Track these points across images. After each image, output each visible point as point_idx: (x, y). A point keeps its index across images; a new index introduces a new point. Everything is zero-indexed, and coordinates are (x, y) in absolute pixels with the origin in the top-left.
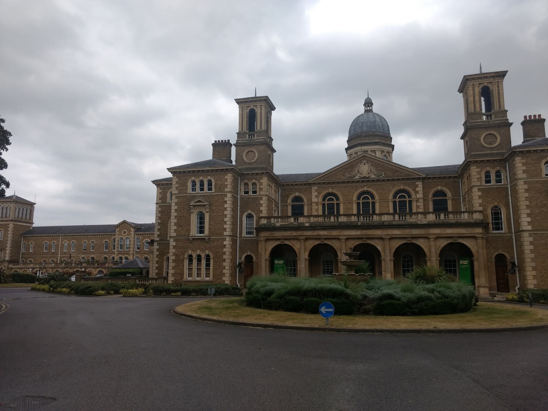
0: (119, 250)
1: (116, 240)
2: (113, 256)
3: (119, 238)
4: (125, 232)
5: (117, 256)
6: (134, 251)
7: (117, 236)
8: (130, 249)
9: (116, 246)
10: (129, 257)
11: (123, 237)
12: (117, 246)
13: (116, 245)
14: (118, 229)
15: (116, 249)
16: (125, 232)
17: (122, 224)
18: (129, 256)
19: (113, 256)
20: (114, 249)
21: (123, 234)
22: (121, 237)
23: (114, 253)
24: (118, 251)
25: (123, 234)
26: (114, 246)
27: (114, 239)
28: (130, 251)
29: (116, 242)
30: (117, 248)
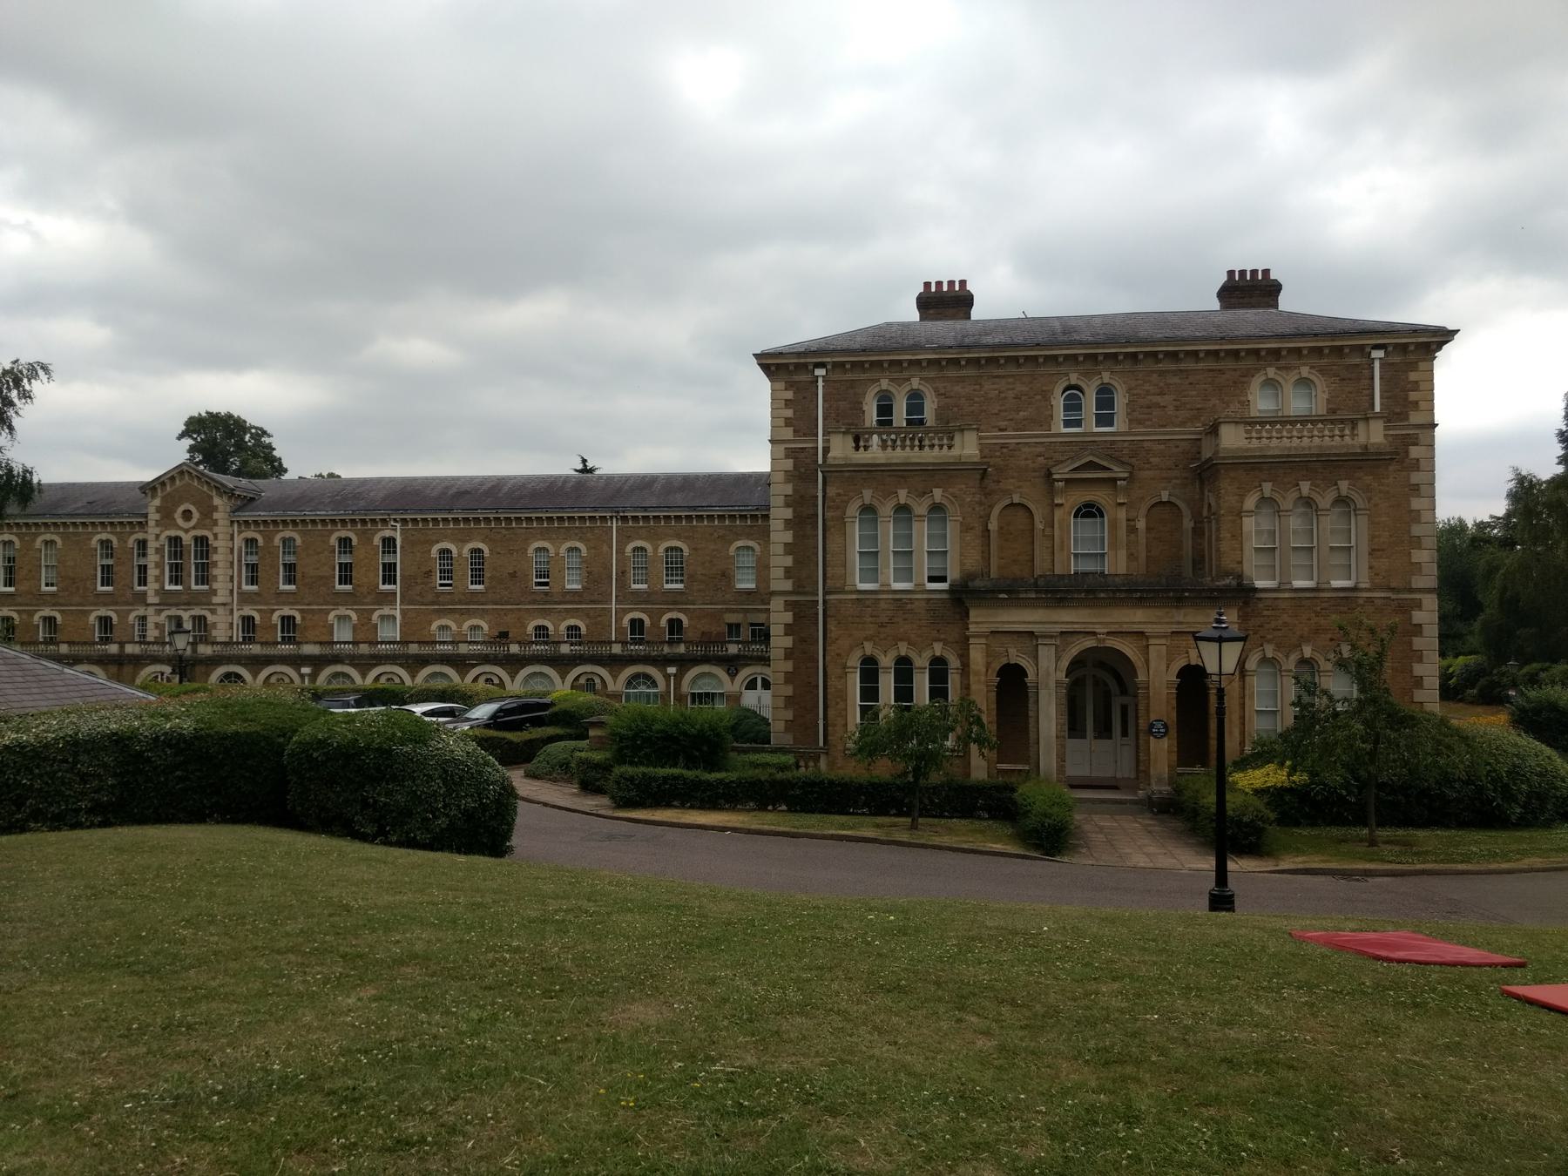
0: (194, 587)
1: (152, 545)
2: (141, 611)
3: (163, 537)
4: (187, 515)
5: (159, 612)
6: (232, 591)
7: (152, 530)
8: (215, 586)
9: (152, 572)
10: (210, 618)
11: (181, 534)
12: (157, 572)
13: (151, 566)
14: (157, 502)
15: (152, 586)
16: (187, 515)
17: (172, 479)
18: (213, 612)
19: (141, 611)
20: (143, 581)
21: (180, 522)
22: (173, 533)
23: (141, 599)
24: (161, 592)
25: (180, 522)
26: (143, 569)
27: (143, 544)
28: (214, 592)
29: (152, 558)
30: (159, 579)
